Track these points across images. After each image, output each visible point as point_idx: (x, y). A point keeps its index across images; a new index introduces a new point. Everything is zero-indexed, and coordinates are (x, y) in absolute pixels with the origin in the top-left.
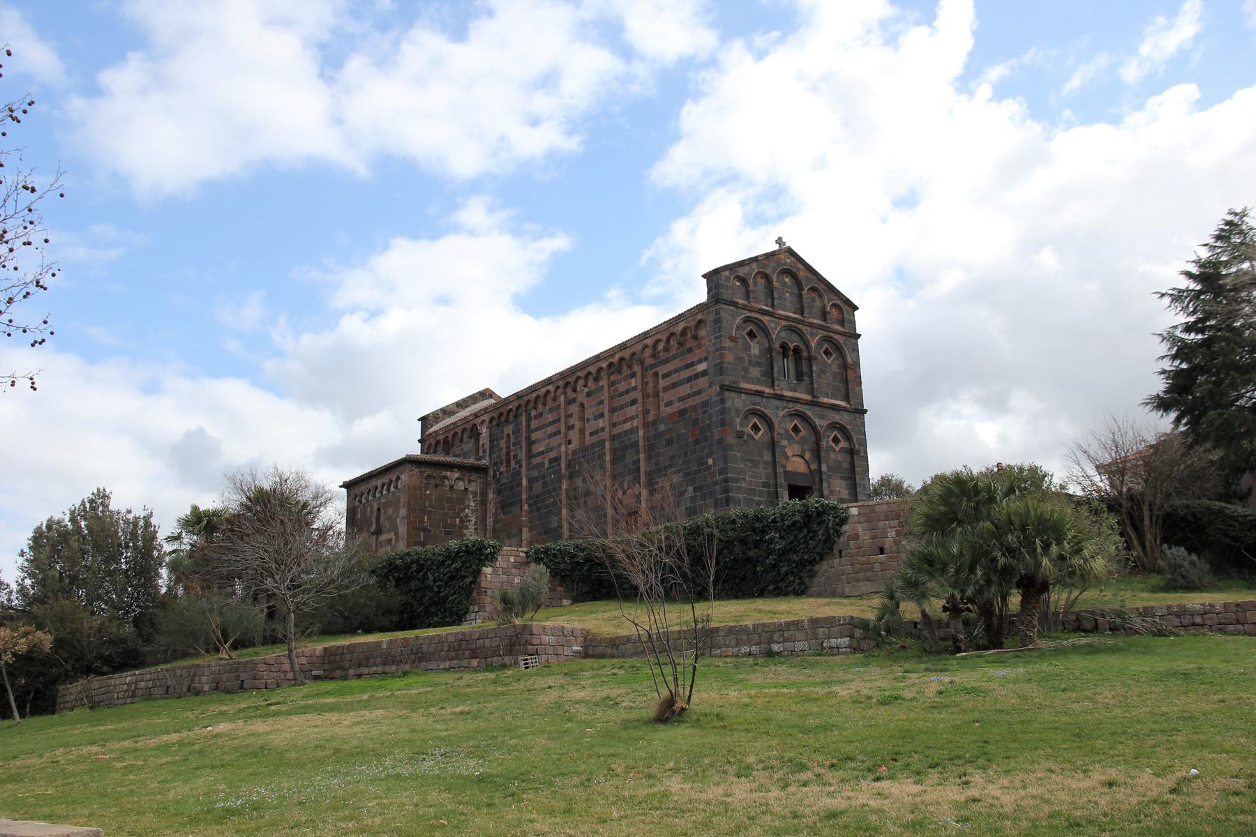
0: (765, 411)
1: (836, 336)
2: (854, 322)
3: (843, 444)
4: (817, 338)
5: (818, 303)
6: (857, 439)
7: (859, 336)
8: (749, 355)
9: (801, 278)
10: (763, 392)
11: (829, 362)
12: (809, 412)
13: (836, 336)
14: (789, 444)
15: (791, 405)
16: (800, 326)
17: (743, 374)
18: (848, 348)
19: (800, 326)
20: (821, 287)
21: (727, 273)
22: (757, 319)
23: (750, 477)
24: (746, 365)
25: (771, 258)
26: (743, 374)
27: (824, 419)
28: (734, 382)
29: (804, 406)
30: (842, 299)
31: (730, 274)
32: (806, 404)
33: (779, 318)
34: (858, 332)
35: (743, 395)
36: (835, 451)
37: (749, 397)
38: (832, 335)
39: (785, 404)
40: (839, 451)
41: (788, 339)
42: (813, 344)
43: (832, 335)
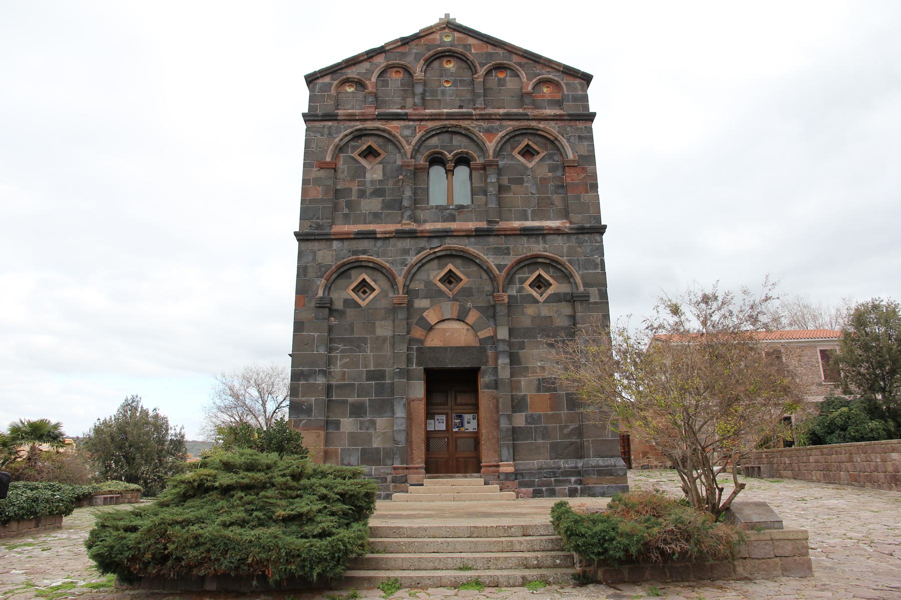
0: (379, 260)
1: (542, 125)
2: (585, 98)
3: (556, 287)
4: (501, 134)
5: (511, 84)
6: (583, 277)
7: (594, 115)
8: (363, 183)
9: (471, 57)
10: (374, 233)
11: (530, 165)
12: (473, 248)
13: (542, 125)
14: (432, 305)
15: (435, 242)
16: (465, 123)
17: (346, 211)
18: (568, 140)
19: (465, 123)
20: (501, 57)
21: (327, 79)
22: (378, 129)
23: (345, 365)
24: (354, 197)
25: (413, 43)
26: (346, 211)
27: (508, 254)
28: (319, 226)
29: (466, 241)
30: (559, 71)
31: (332, 80)
32: (468, 236)
33: (422, 120)
34: (591, 110)
35: (335, 242)
36: (536, 301)
37: (346, 243)
38: (534, 124)
39: (423, 243)
40: (545, 302)
41: (443, 147)
42: (491, 146)
43: (534, 124)
